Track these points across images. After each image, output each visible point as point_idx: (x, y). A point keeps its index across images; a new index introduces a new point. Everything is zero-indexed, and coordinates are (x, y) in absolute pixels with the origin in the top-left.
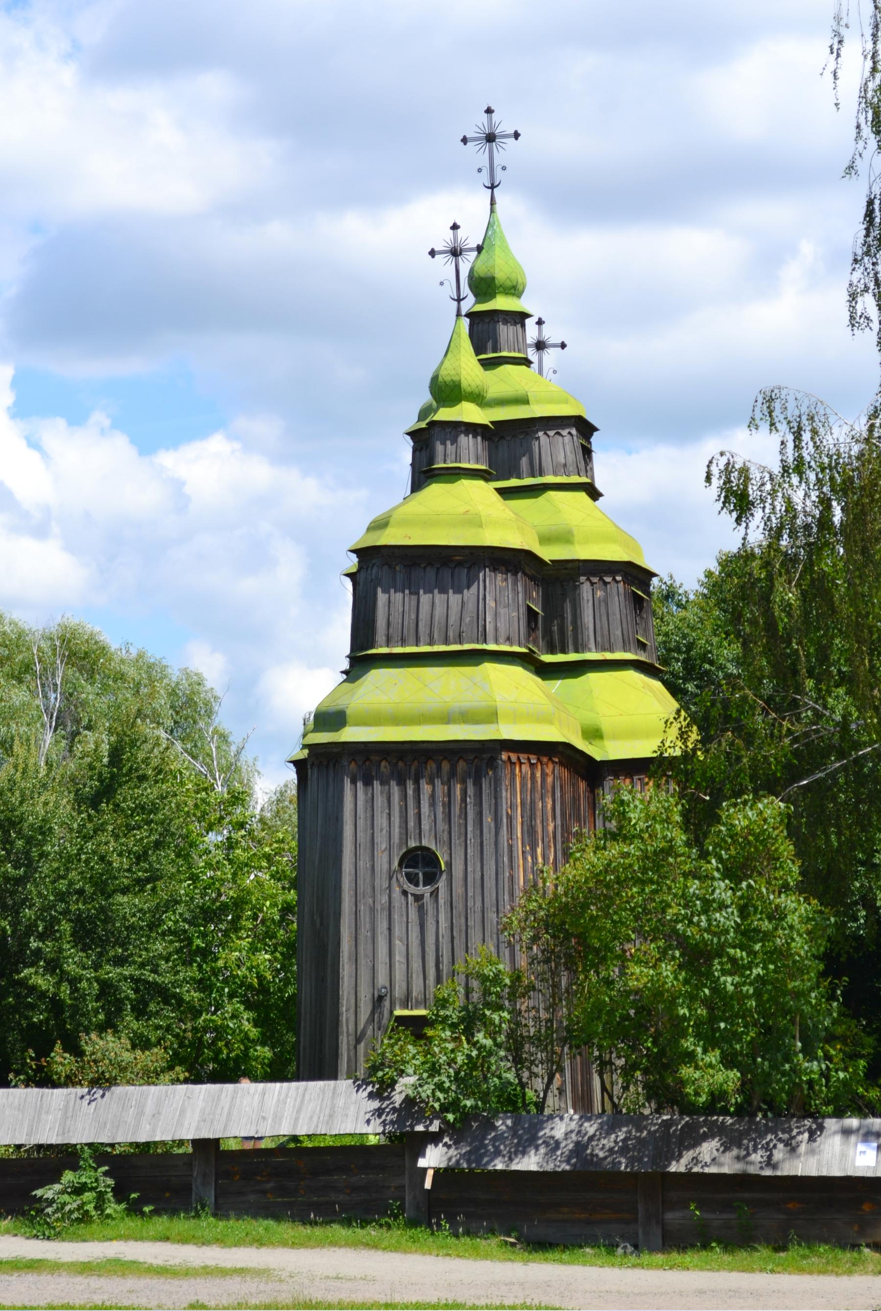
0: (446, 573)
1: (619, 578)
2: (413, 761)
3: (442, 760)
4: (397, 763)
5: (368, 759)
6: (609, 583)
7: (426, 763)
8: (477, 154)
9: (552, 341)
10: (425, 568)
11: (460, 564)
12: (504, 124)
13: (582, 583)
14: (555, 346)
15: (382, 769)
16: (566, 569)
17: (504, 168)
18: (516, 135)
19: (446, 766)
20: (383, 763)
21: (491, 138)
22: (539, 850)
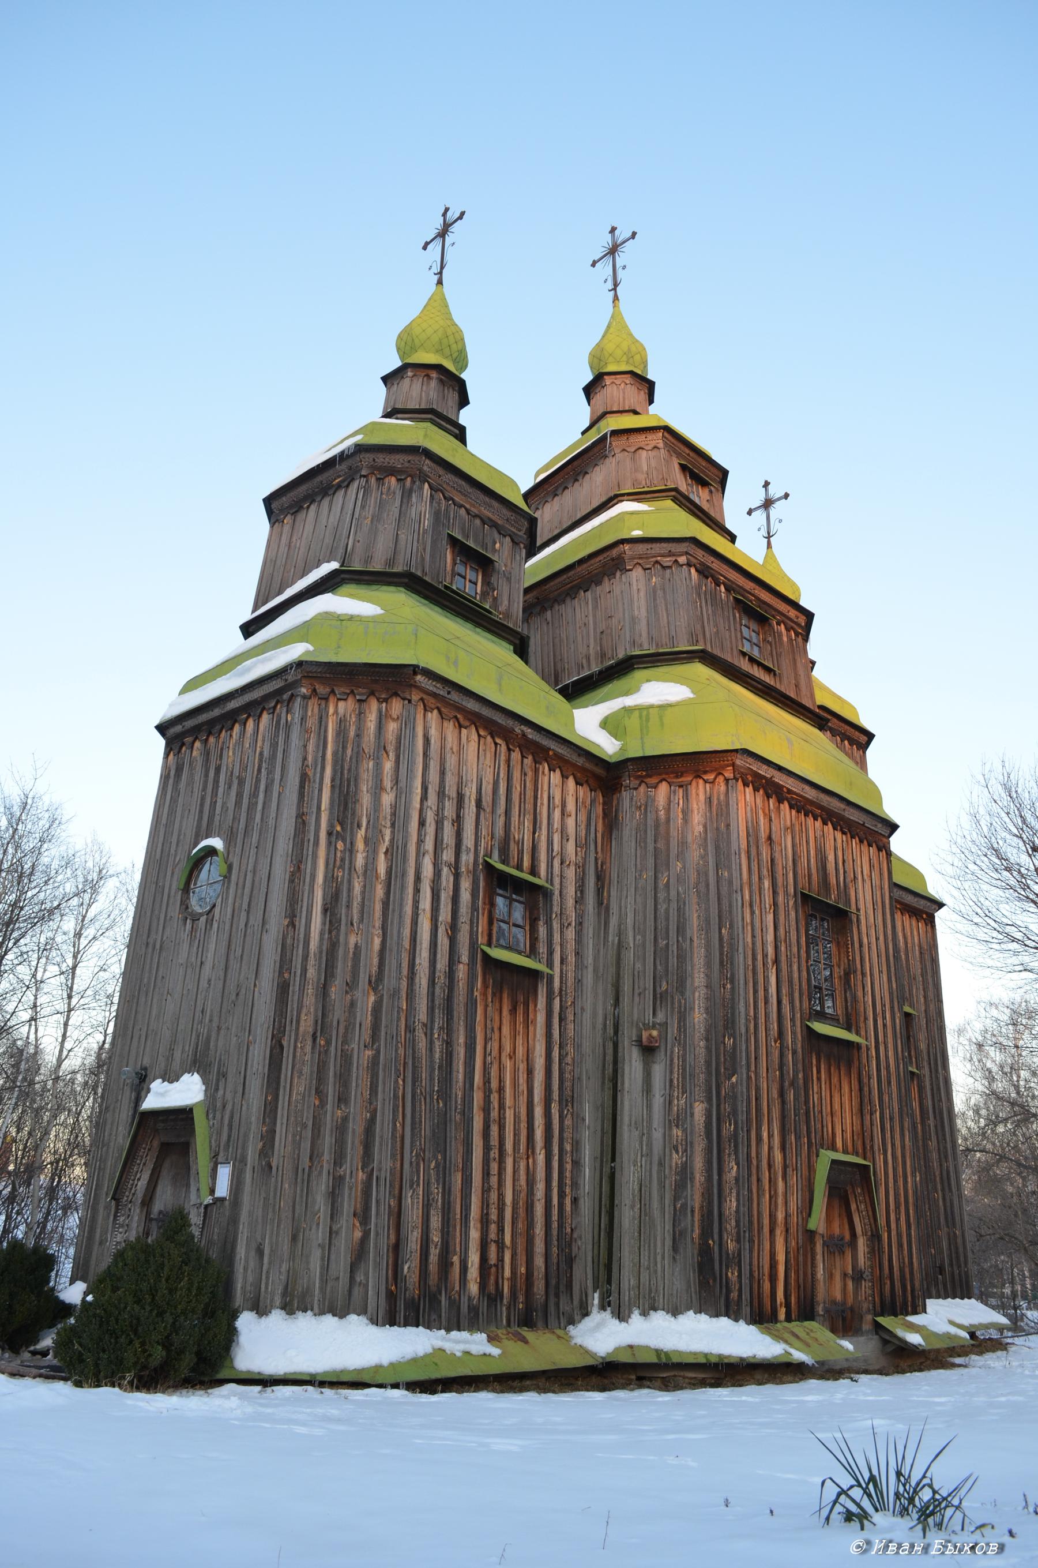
0: (326, 502)
1: (682, 560)
2: (221, 731)
3: (247, 719)
4: (206, 740)
5: (183, 744)
6: (670, 567)
7: (232, 729)
8: (605, 269)
9: (777, 496)
10: (308, 507)
11: (339, 487)
12: (622, 234)
13: (630, 570)
14: (779, 499)
15: (195, 753)
16: (613, 559)
17: (624, 268)
18: (634, 235)
19: (250, 724)
20: (198, 744)
21: (613, 250)
22: (361, 833)
